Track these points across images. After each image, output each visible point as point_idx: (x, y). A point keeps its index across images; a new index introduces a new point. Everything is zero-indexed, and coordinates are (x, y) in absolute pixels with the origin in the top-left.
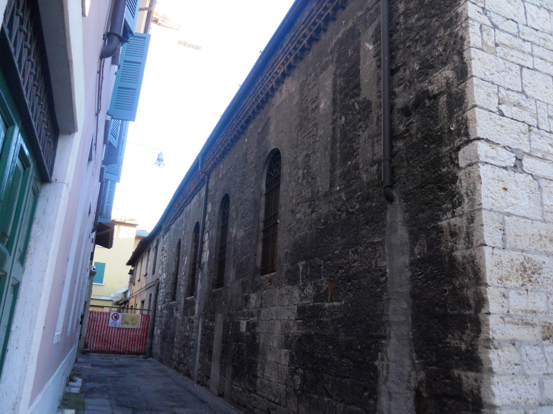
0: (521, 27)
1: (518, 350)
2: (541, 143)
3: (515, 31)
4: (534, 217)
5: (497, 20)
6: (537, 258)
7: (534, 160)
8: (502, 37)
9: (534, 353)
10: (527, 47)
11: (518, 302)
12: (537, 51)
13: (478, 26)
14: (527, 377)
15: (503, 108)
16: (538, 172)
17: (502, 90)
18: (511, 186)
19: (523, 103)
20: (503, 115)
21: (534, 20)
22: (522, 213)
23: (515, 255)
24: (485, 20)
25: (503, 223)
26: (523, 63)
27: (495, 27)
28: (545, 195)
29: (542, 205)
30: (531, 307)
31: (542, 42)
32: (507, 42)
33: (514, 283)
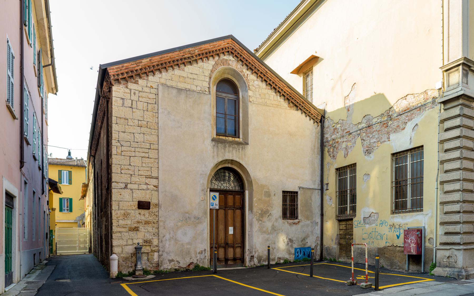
0: (132, 143)
1: (121, 234)
2: (134, 179)
3: (129, 145)
4: (129, 200)
5: (123, 143)
6: (129, 211)
7: (131, 185)
8: (124, 148)
9: (126, 234)
10: (133, 149)
11: (121, 222)
12: (137, 149)
13: (115, 147)
14: (123, 239)
15: (122, 171)
16: (132, 188)
17: (122, 166)
18: (123, 193)
19: (129, 168)
20: (121, 173)
21: (137, 139)
22: (125, 200)
23: (122, 211)
24: (119, 144)
25: (119, 203)
26: (130, 155)
27: (122, 146)
28: (134, 195)
29: (133, 197)
30: (126, 223)
31: (139, 146)
32: (126, 150)
33: (121, 218)
